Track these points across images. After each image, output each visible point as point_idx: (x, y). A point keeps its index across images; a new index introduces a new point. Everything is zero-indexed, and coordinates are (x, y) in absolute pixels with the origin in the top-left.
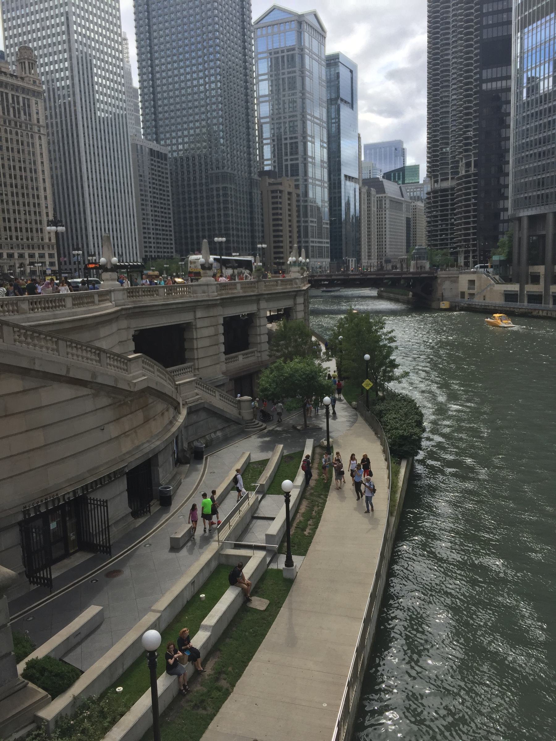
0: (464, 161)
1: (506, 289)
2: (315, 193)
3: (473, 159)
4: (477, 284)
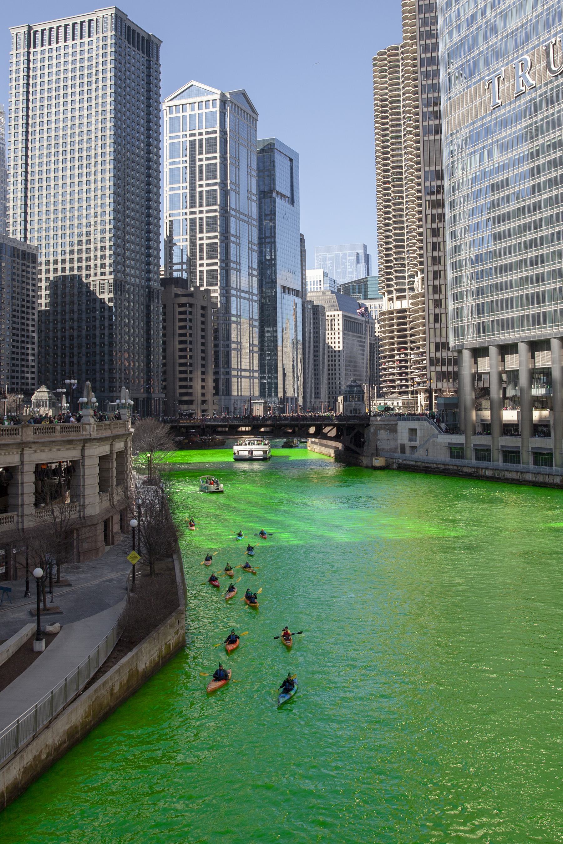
2: (239, 308)
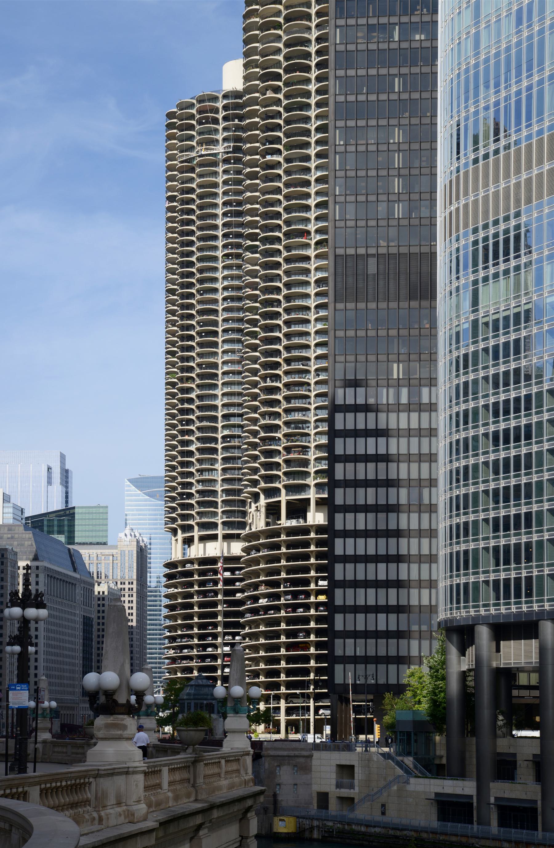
1: (439, 790)
4: (359, 773)
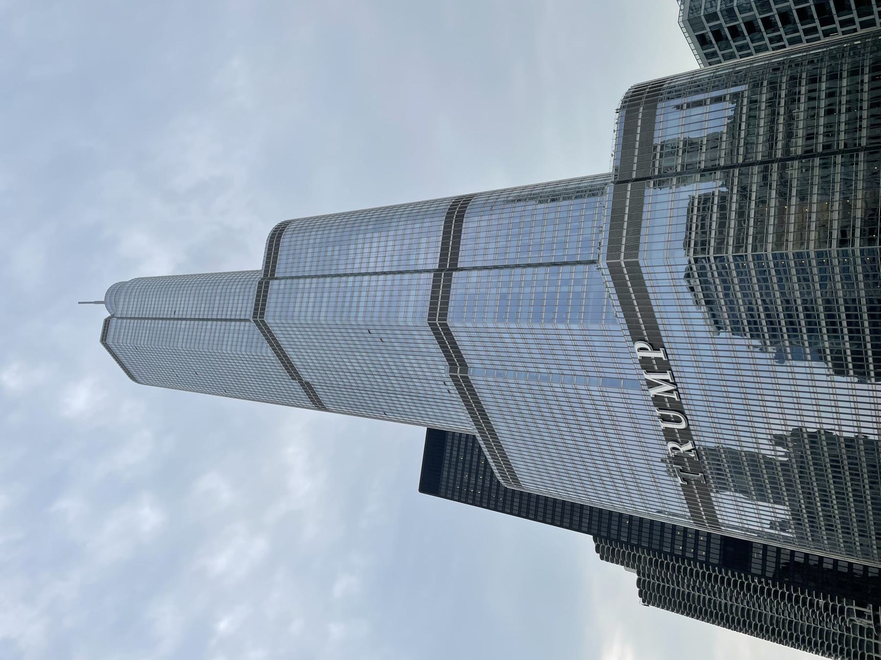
0: (855, 618)
3: (855, 608)
